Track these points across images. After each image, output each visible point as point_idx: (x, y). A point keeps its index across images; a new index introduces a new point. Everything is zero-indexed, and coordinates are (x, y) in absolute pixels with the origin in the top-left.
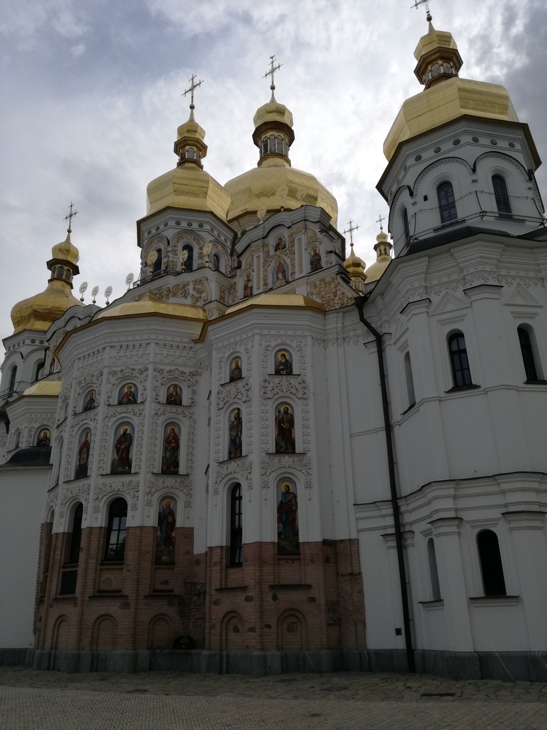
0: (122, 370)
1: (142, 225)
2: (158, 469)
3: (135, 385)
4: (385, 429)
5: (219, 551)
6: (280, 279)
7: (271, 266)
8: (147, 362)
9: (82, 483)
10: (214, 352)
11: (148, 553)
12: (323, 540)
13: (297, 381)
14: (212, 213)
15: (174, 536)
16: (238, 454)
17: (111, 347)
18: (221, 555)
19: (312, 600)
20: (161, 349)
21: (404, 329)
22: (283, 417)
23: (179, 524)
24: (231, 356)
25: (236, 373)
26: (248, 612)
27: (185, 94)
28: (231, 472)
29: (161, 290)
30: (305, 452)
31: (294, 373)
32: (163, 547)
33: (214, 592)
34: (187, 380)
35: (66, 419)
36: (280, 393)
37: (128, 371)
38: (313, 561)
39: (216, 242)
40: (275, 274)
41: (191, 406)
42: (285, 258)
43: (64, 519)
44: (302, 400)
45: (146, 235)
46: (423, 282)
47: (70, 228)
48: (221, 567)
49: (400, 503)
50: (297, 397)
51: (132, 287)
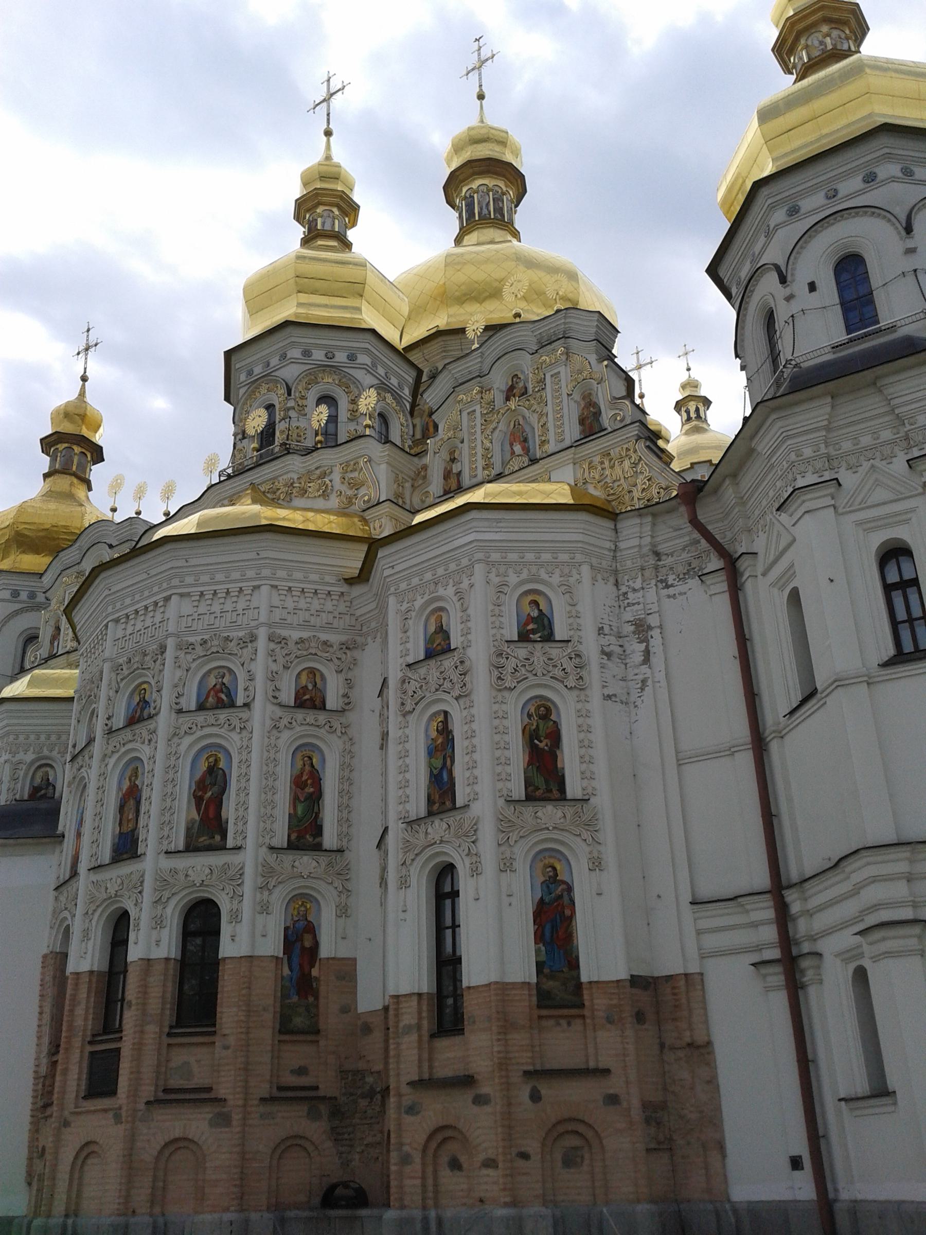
0: (204, 642)
1: (234, 358)
2: (281, 838)
3: (230, 670)
4: (750, 746)
5: (414, 1002)
6: (518, 456)
7: (498, 430)
8: (253, 624)
9: (127, 869)
10: (392, 600)
11: (264, 1010)
12: (632, 976)
13: (565, 654)
14: (373, 332)
15: (318, 976)
16: (447, 803)
17: (182, 595)
18: (420, 1012)
19: (612, 1100)
20: (283, 597)
21: (783, 544)
22: (537, 726)
23: (325, 951)
24: (428, 606)
25: (437, 642)
26: (479, 1128)
27: (314, 108)
28: (433, 841)
29: (276, 484)
30: (586, 797)
31: (558, 637)
32: (295, 999)
33: (405, 1089)
34: (336, 661)
35: (90, 741)
36: (531, 677)
37: (216, 642)
38: (610, 1020)
39: (383, 388)
40: (507, 447)
41: (344, 711)
43: (91, 943)
44: (576, 692)
45: (243, 377)
46: (823, 446)
47: (85, 372)
48: (420, 1036)
49: (791, 896)
50: (566, 686)
51: (215, 480)
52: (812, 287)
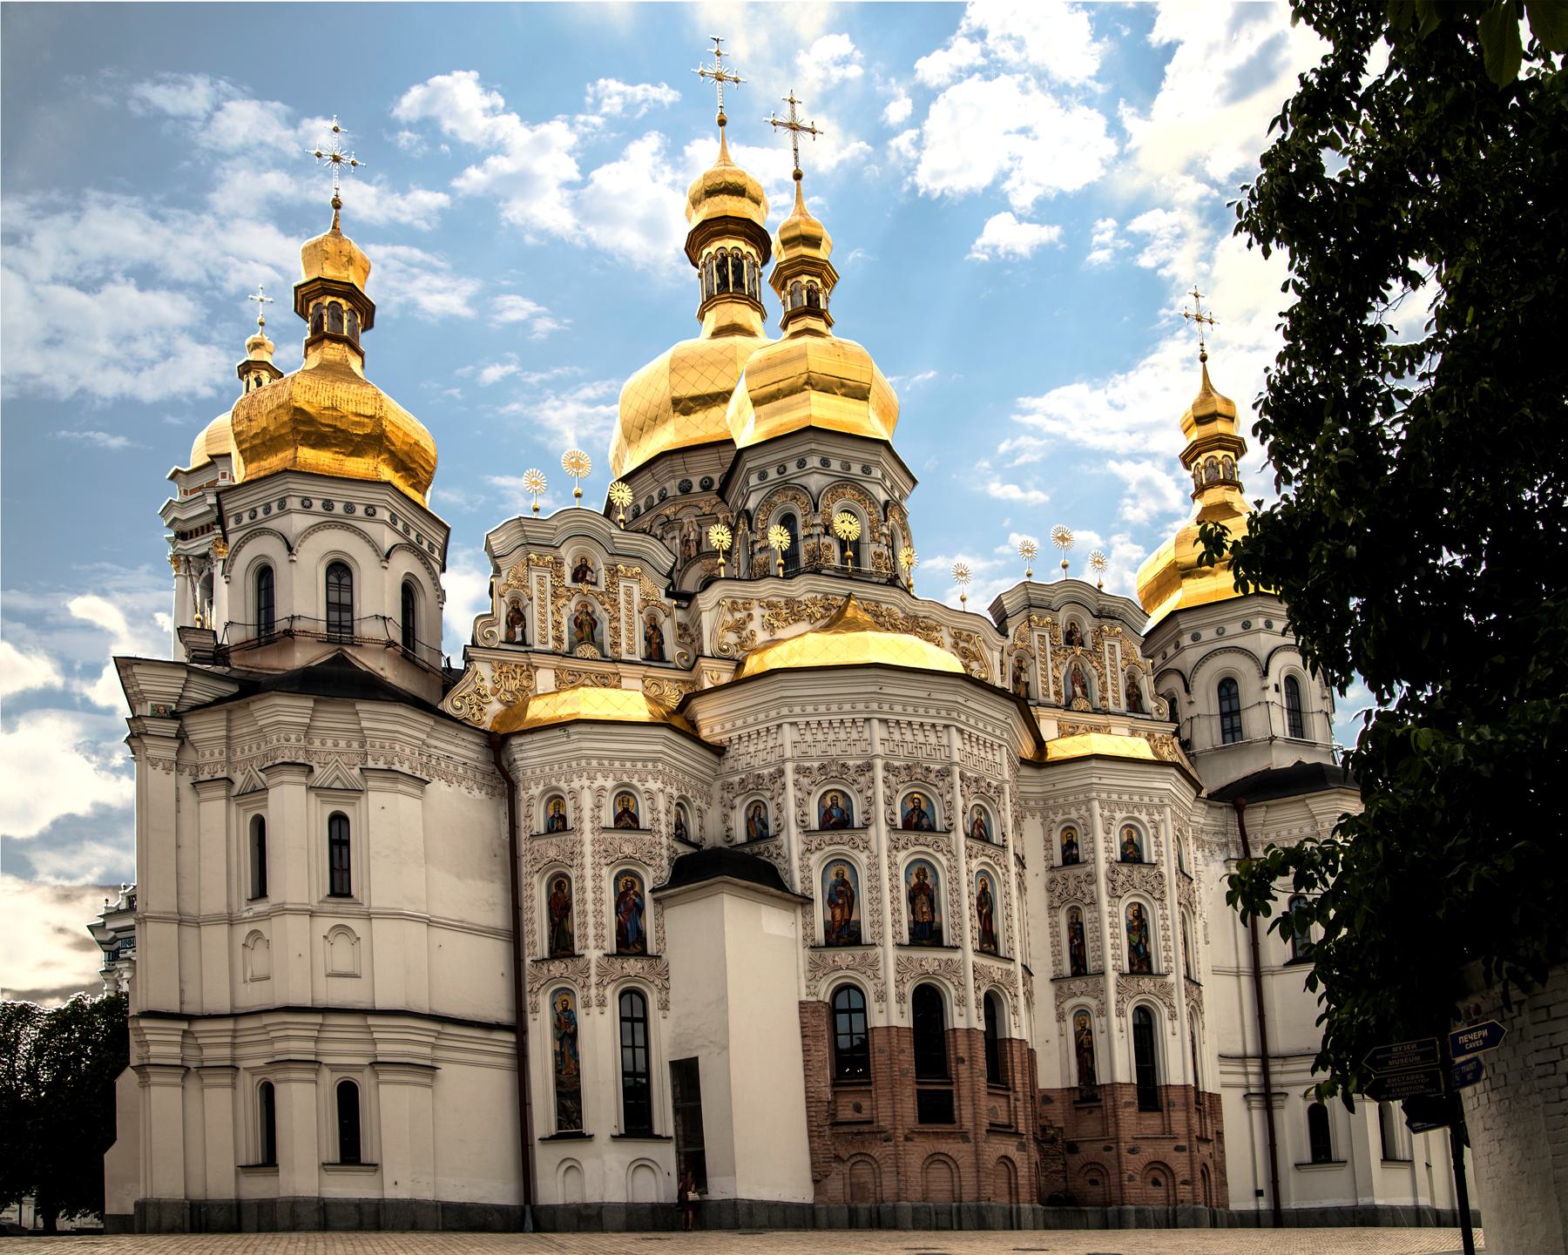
0: (976, 781)
10: (1096, 804)
40: (1069, 684)
42: (1089, 666)
52: (1277, 689)
